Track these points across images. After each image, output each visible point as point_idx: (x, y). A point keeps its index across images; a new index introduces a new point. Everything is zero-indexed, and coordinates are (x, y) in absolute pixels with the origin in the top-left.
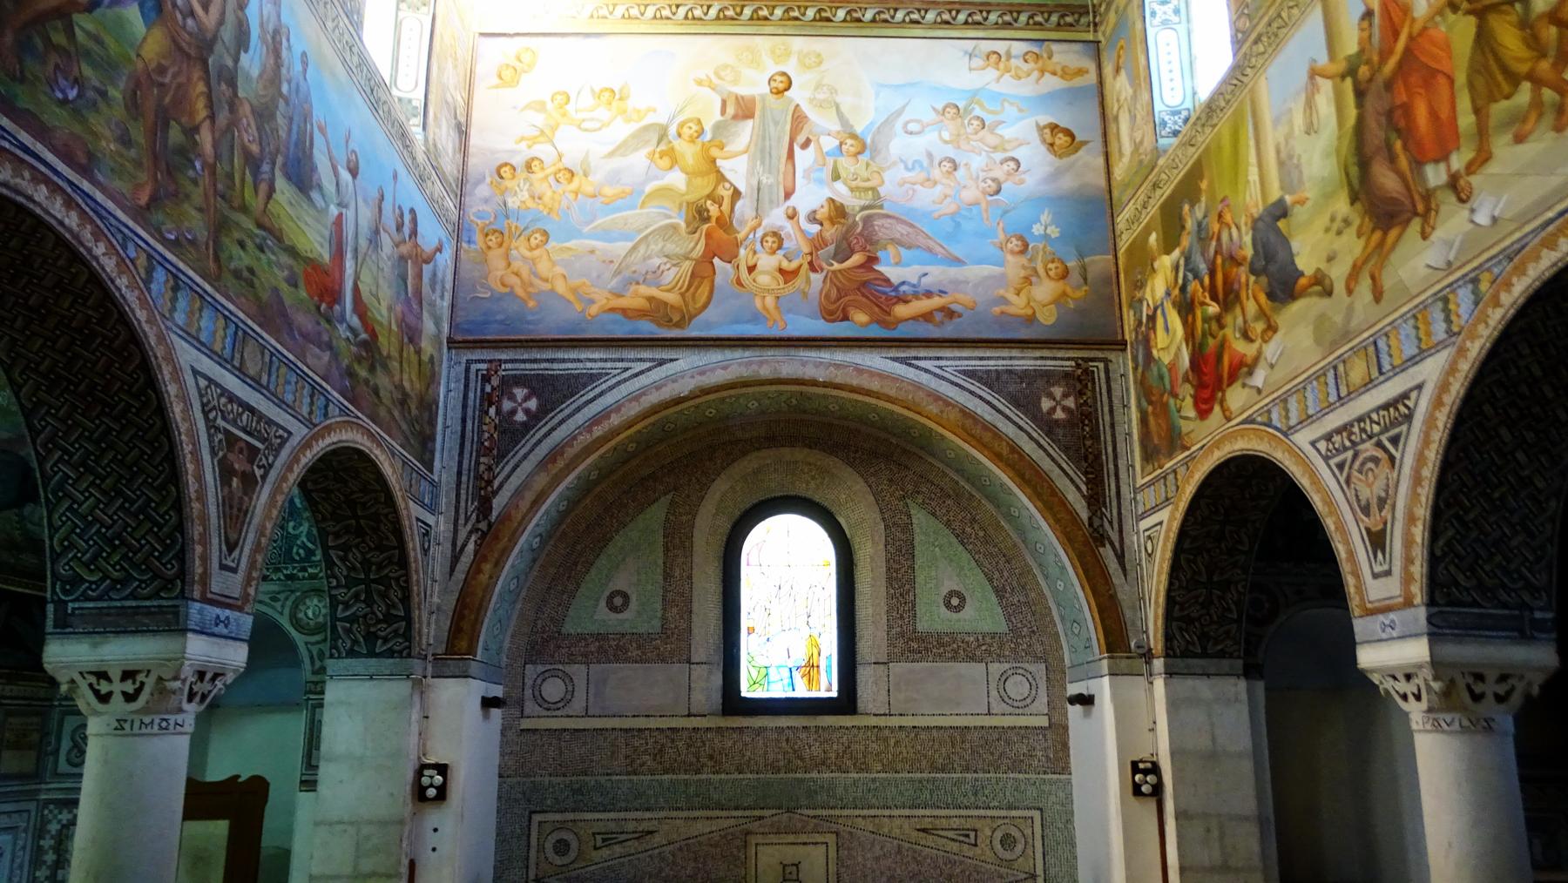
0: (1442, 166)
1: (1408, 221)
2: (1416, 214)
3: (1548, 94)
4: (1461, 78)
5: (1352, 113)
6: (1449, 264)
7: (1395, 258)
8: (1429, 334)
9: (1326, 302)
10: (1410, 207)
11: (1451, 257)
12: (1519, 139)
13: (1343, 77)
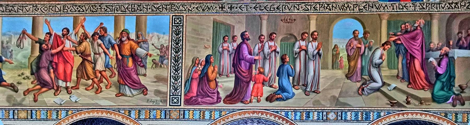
0: (65, 83)
1: (50, 89)
2: (53, 88)
3: (95, 85)
4: (75, 69)
5: (37, 53)
6: (61, 104)
7: (44, 95)
8: (51, 116)
9: (14, 93)
10: (52, 85)
11: (62, 103)
12: (86, 89)
13: (36, 42)
